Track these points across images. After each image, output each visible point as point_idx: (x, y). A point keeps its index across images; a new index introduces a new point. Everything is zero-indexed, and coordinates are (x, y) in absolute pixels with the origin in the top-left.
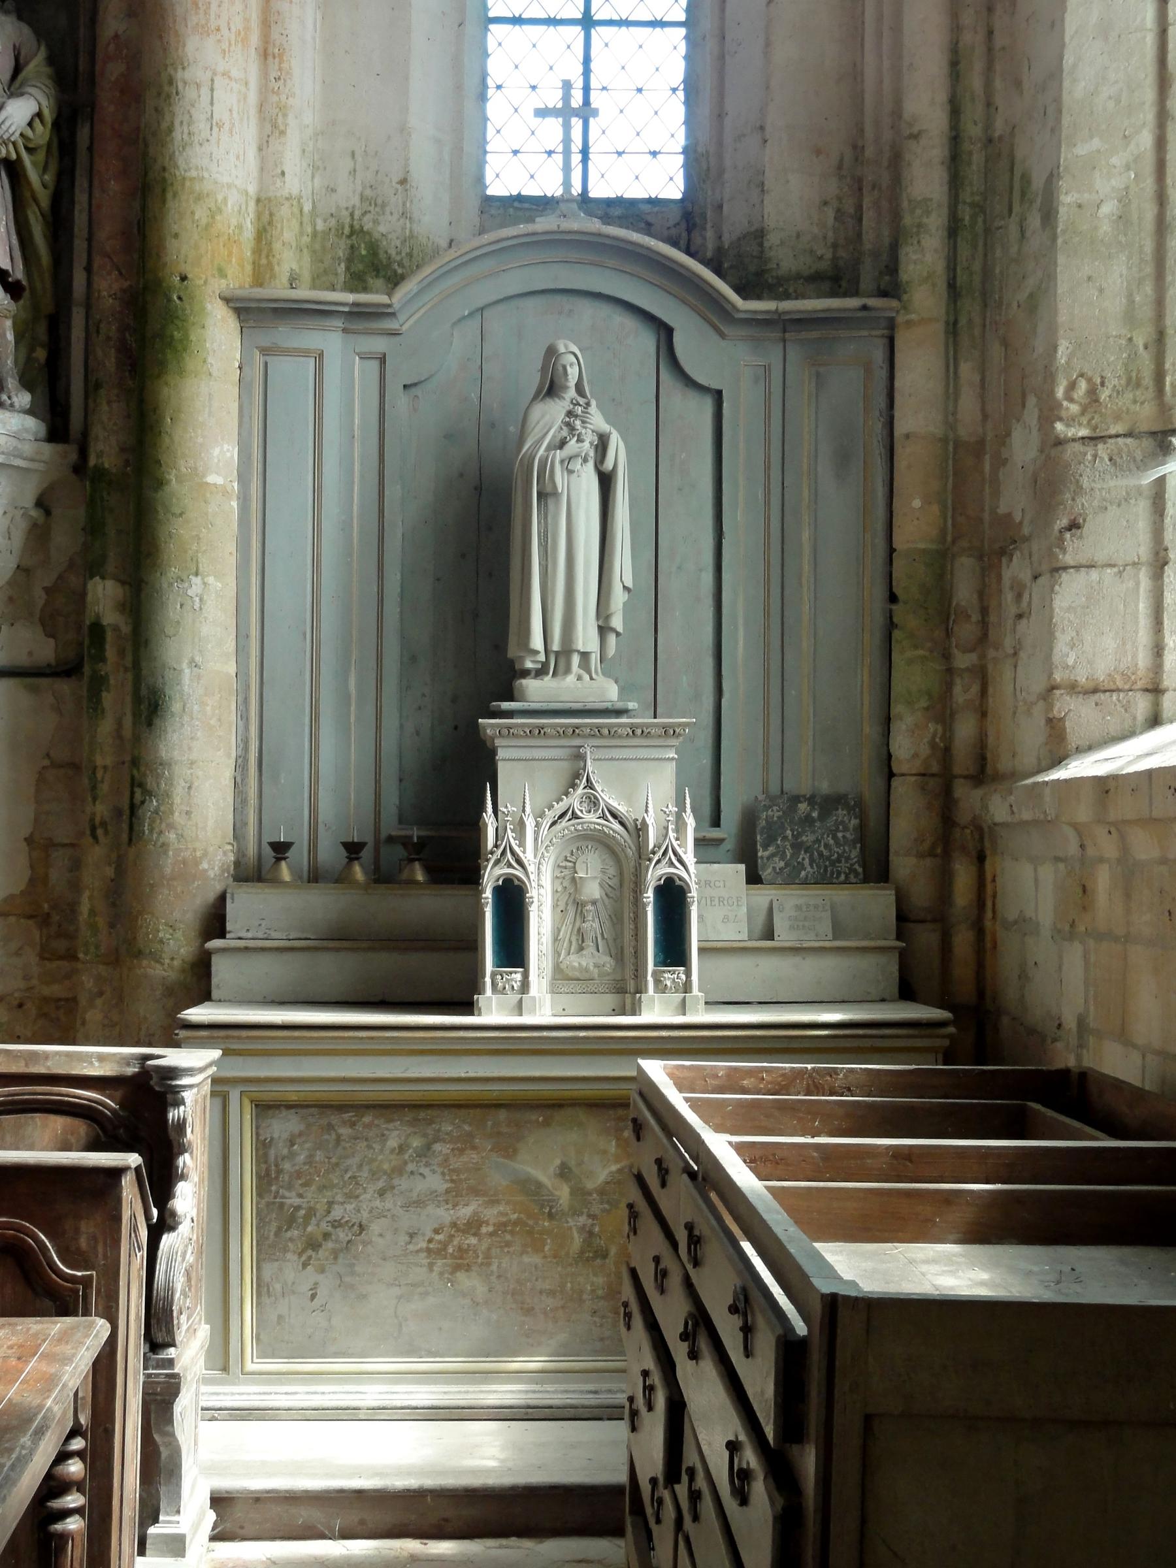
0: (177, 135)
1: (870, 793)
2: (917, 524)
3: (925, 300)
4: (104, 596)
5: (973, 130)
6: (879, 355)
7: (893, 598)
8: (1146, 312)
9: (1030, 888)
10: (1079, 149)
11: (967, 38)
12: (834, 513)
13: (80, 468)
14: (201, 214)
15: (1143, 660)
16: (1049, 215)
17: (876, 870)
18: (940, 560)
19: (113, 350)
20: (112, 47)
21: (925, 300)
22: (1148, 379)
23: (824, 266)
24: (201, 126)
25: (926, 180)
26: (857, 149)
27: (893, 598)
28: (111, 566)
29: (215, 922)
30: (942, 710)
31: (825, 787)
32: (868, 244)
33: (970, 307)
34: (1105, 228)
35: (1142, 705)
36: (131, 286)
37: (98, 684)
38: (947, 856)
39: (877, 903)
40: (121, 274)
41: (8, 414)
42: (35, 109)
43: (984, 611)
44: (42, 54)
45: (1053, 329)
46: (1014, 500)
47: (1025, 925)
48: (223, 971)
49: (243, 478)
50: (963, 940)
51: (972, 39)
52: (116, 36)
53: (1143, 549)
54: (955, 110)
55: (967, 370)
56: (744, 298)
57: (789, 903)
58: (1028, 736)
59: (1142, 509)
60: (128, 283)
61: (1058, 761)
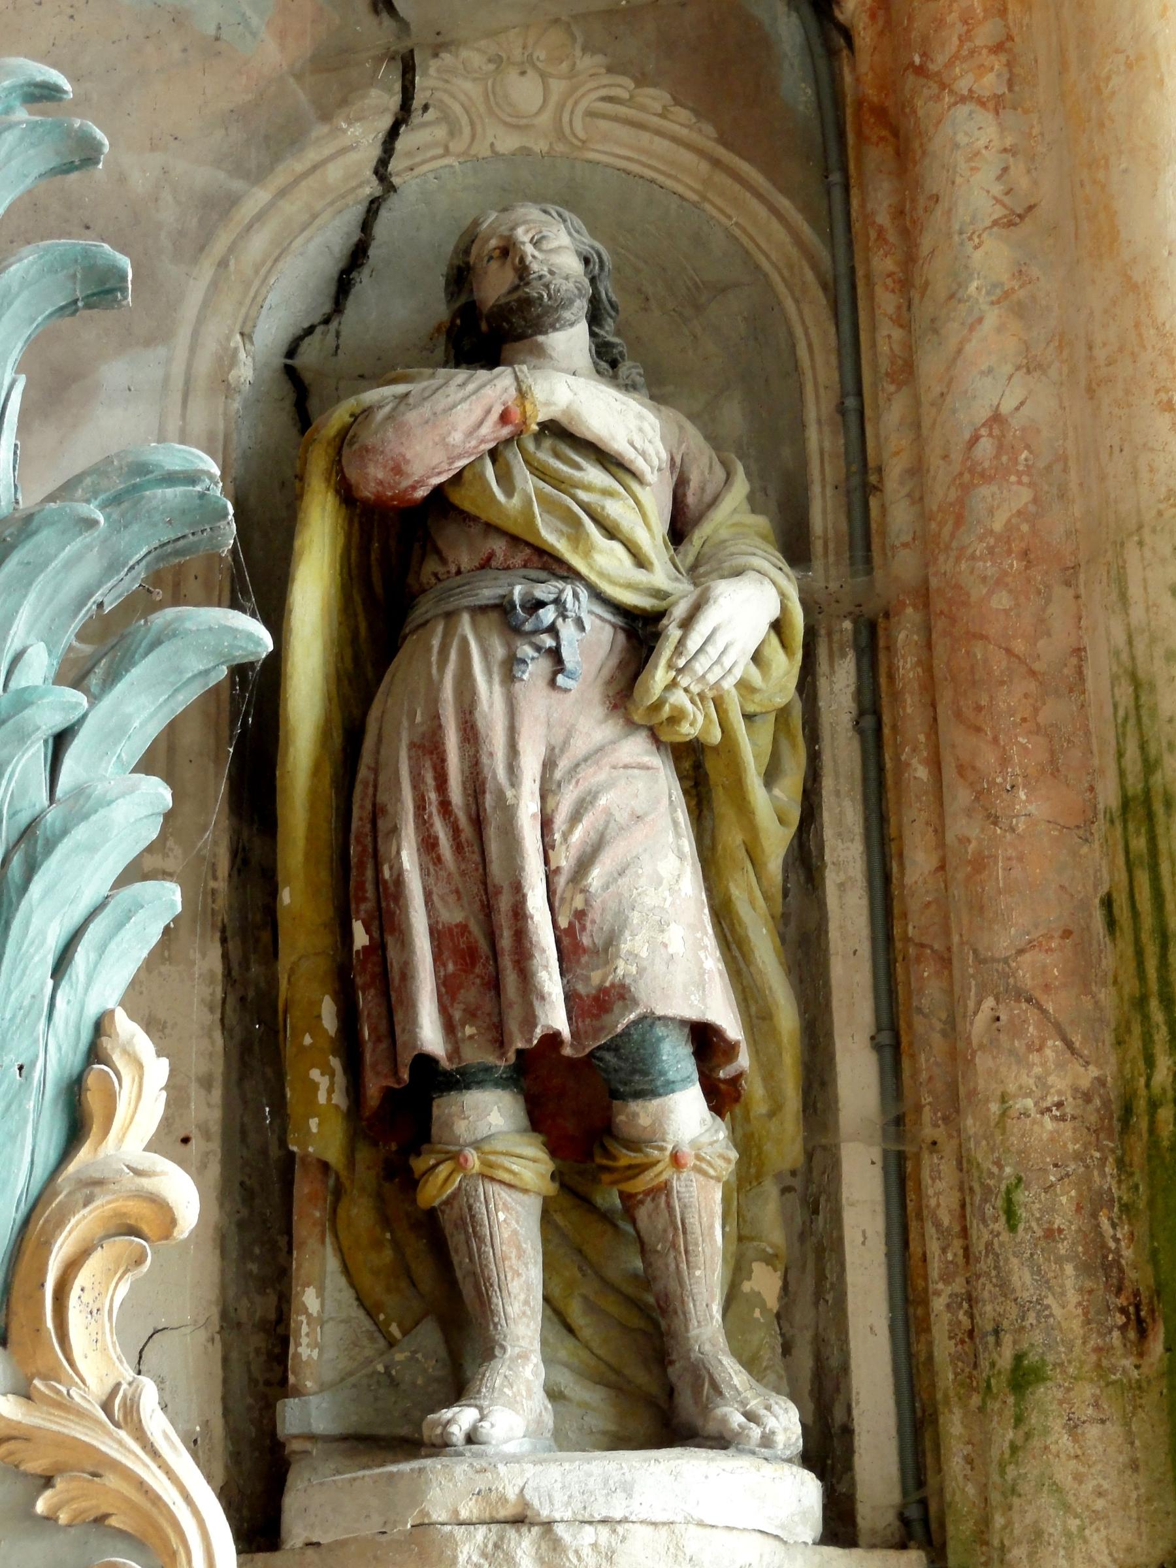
19: (1069, 1269)
20: (986, 446)
36: (1101, 1081)
40: (1069, 1045)
41: (769, 1469)
42: (774, 612)
44: (741, 487)
52: (997, 418)
60: (1093, 1071)
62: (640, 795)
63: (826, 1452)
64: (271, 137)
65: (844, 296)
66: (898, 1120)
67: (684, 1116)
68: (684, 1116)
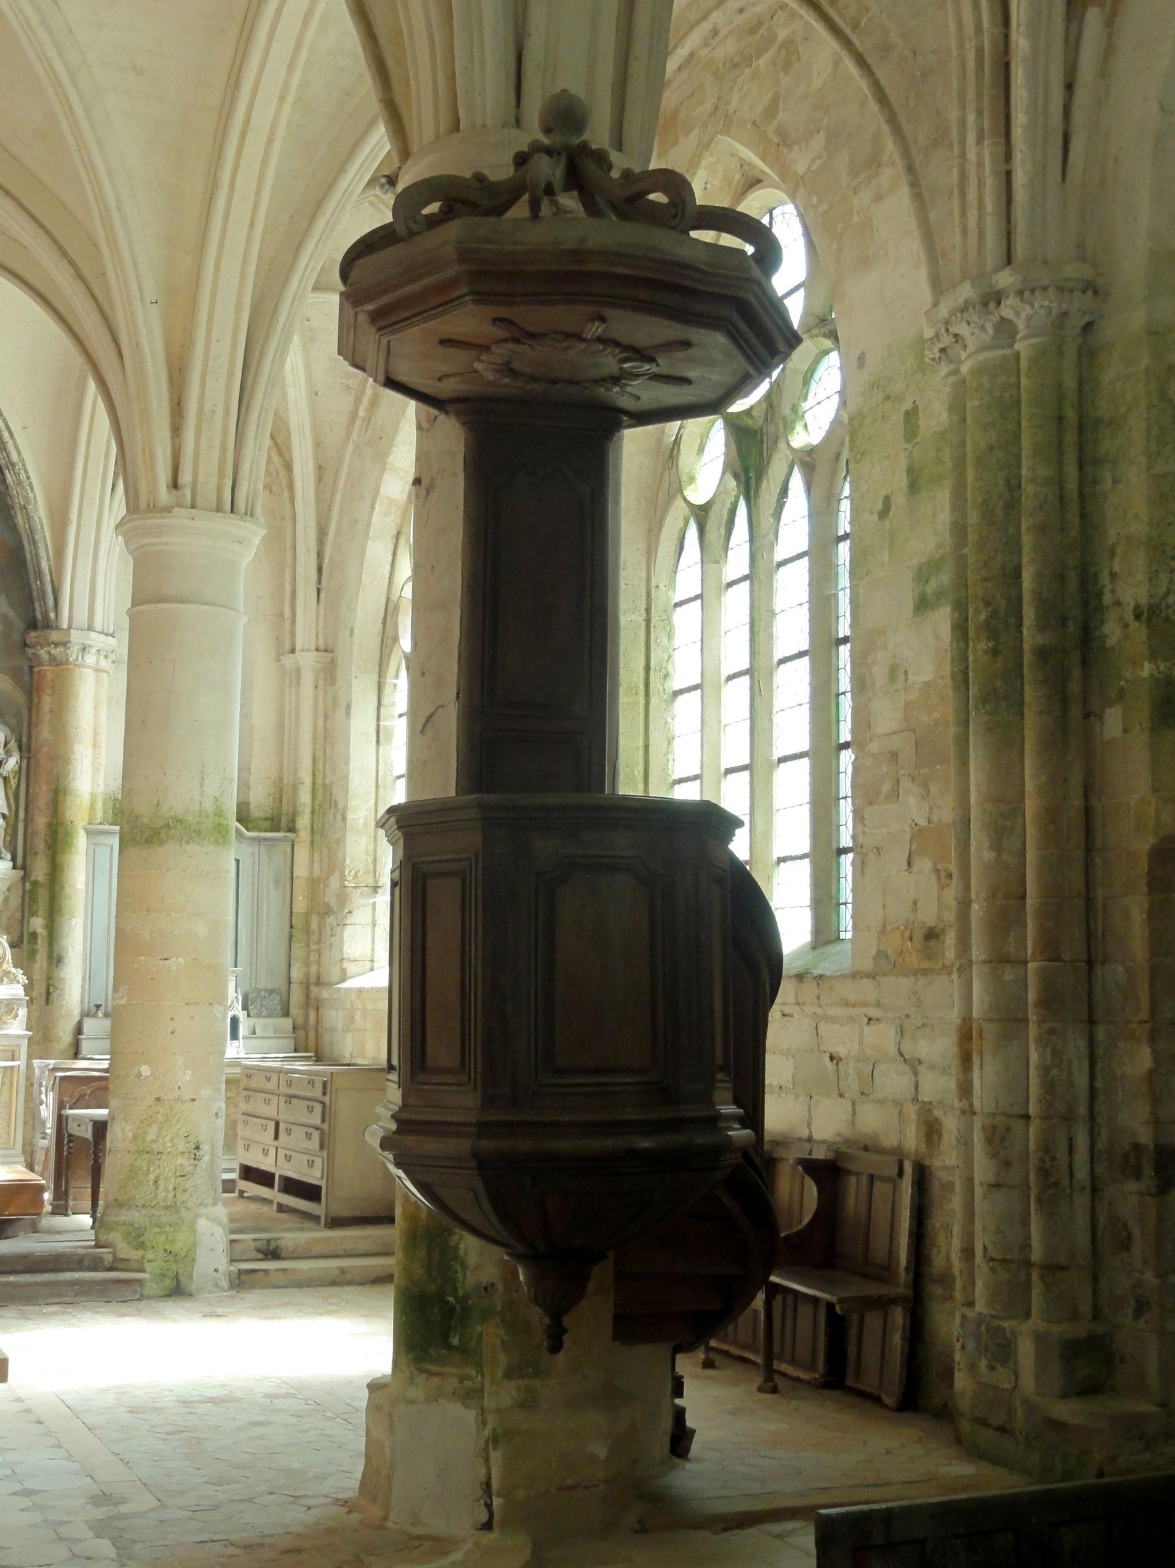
0: (71, 775)
1: (284, 988)
3: (304, 834)
4: (38, 924)
5: (319, 782)
6: (289, 850)
7: (292, 927)
8: (372, 852)
9: (334, 1018)
10: (353, 803)
11: (318, 753)
12: (274, 899)
13: (24, 879)
14: (78, 802)
15: (369, 952)
16: (344, 819)
17: (286, 1014)
18: (307, 915)
21: (304, 834)
22: (371, 871)
23: (269, 815)
24: (79, 772)
25: (305, 797)
26: (281, 778)
27: (292, 927)
28: (40, 912)
29: (79, 1030)
30: (307, 963)
31: (269, 986)
32: (284, 810)
34: (361, 826)
35: (368, 965)
37: (32, 953)
38: (307, 1008)
39: (287, 1023)
43: (320, 931)
45: (344, 853)
46: (332, 900)
47: (333, 1029)
48: (85, 1046)
49: (87, 885)
53: (370, 921)
54: (314, 775)
55: (316, 857)
56: (248, 830)
57: (260, 1023)
58: (335, 973)
59: (370, 909)
61: (344, 980)
63: (14, 859)
65: (30, 709)
66: (26, 821)
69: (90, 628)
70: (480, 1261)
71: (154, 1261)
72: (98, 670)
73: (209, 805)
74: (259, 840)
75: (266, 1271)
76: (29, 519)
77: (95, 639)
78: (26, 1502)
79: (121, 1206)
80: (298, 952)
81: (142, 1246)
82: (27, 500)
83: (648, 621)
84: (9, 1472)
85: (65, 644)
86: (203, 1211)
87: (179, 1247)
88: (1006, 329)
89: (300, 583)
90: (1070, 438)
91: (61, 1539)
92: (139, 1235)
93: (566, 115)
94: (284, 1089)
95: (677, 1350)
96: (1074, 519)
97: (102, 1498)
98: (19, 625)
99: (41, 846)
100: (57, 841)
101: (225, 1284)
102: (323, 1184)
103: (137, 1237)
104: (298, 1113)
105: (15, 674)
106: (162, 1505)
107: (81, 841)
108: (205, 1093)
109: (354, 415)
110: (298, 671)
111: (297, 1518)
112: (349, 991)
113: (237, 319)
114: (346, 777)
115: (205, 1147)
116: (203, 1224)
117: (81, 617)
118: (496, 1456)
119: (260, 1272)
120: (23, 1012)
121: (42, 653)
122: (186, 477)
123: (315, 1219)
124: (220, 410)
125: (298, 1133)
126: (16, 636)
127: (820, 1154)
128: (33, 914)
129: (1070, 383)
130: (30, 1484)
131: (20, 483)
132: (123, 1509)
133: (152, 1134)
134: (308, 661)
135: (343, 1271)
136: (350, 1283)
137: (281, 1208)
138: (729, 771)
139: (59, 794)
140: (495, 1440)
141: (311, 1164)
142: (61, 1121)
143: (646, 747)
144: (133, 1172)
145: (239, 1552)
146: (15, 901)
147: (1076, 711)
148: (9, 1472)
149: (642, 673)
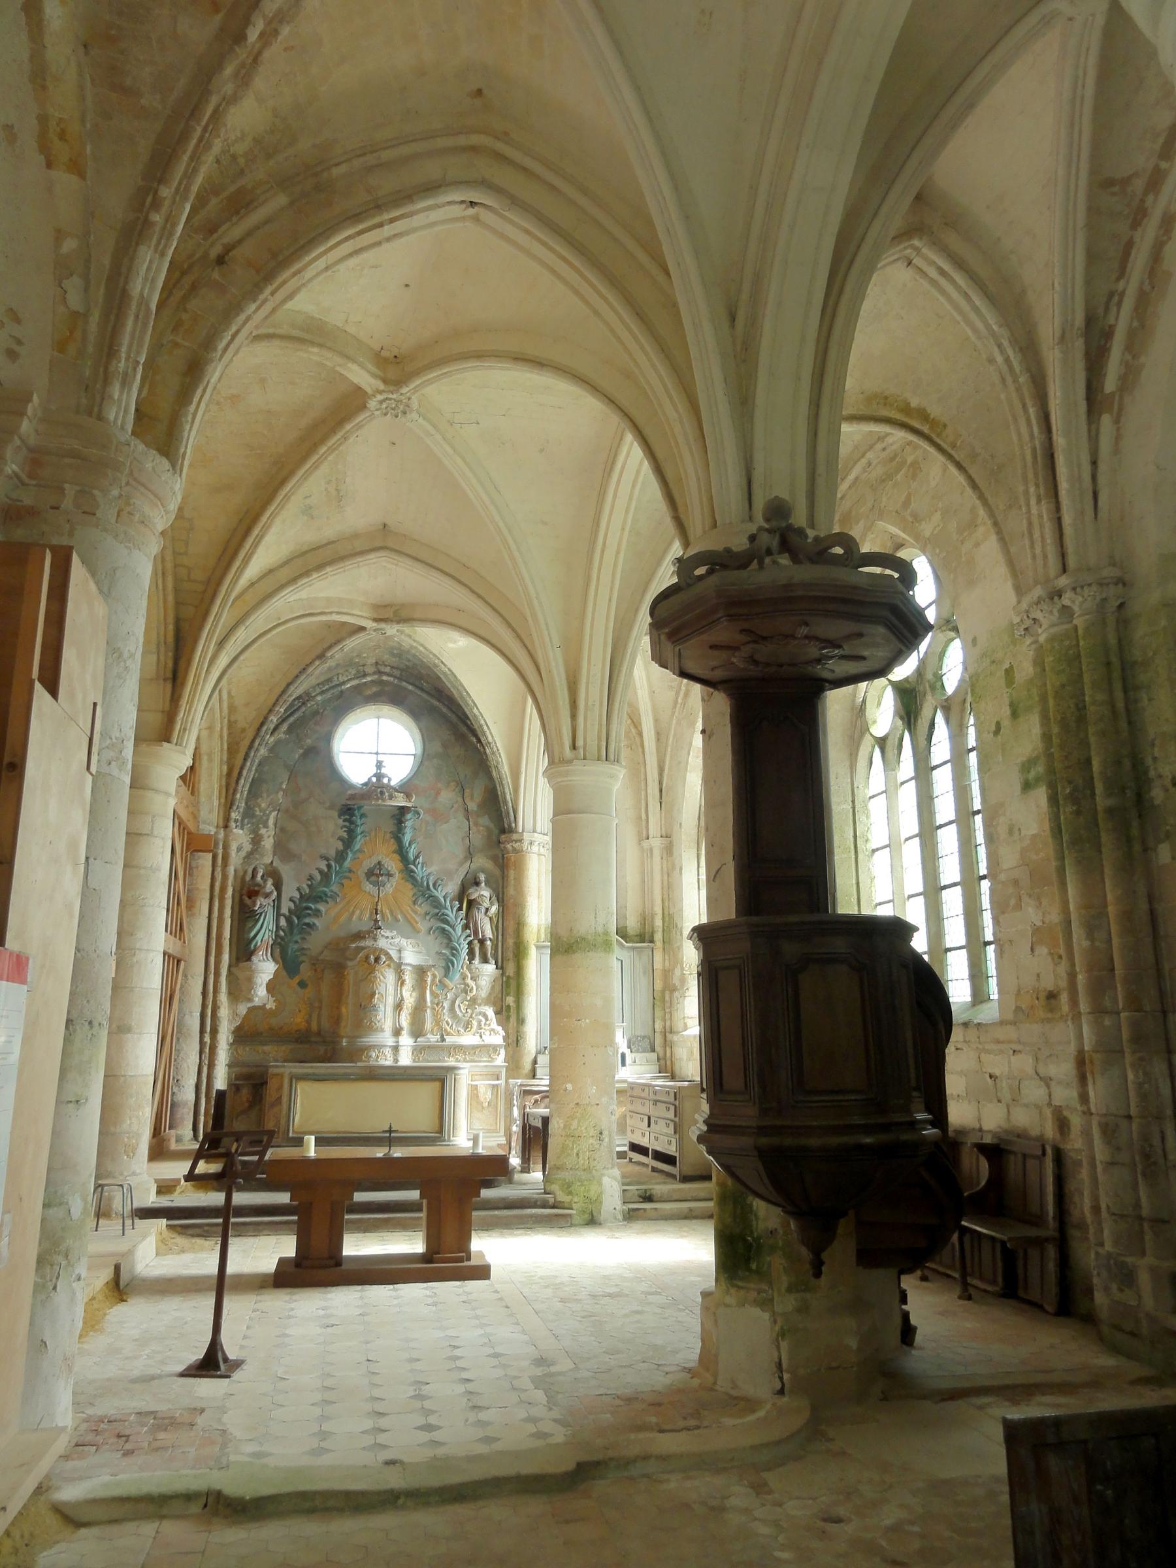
1: (651, 1035)
2: (659, 985)
3: (659, 943)
4: (510, 1000)
12: (643, 982)
13: (503, 974)
17: (653, 1050)
18: (663, 992)
25: (658, 922)
29: (535, 1062)
30: (664, 1020)
33: (667, 945)
37: (508, 1017)
39: (654, 1056)
46: (676, 981)
50: (669, 1063)
51: (666, 896)
57: (638, 1056)
58: (680, 1026)
62: (487, 920)
63: (496, 963)
64: (461, 864)
67: (489, 943)
68: (489, 943)
69: (534, 831)
70: (767, 1216)
71: (578, 1203)
72: (539, 855)
73: (600, 929)
74: (634, 948)
75: (645, 1210)
76: (499, 773)
77: (537, 837)
78: (495, 1362)
79: (558, 1168)
80: (658, 1013)
81: (570, 1193)
82: (498, 762)
83: (854, 808)
84: (487, 1340)
85: (520, 841)
86: (606, 1172)
87: (592, 1194)
88: (1066, 611)
89: (650, 799)
90: (1116, 674)
91: (514, 1389)
92: (569, 1187)
93: (778, 510)
94: (652, 1097)
95: (902, 1272)
96: (1123, 725)
97: (541, 1361)
98: (497, 831)
99: (510, 955)
100: (519, 952)
101: (620, 1217)
102: (677, 1155)
103: (568, 1187)
104: (661, 1111)
105: (494, 859)
106: (577, 1368)
107: (533, 952)
108: (604, 1100)
109: (676, 702)
110: (651, 850)
111: (660, 1381)
112: (688, 1036)
113: (605, 651)
114: (682, 910)
115: (606, 1133)
116: (606, 1180)
117: (529, 825)
118: (784, 1345)
119: (641, 1208)
120: (503, 1052)
121: (509, 846)
122: (580, 742)
123: (673, 1176)
124: (597, 704)
125: (662, 1123)
126: (494, 838)
127: (988, 1140)
128: (508, 994)
129: (1113, 641)
130: (499, 1350)
131: (493, 753)
132: (553, 1369)
133: (575, 1124)
134: (656, 843)
135: (691, 1210)
136: (696, 1218)
137: (654, 1169)
138: (910, 897)
139: (520, 926)
140: (782, 1334)
141: (670, 1143)
142: (525, 1116)
143: (858, 883)
144: (564, 1148)
145: (622, 1403)
146: (498, 988)
147: (1137, 847)
148: (487, 1340)
149: (852, 839)
